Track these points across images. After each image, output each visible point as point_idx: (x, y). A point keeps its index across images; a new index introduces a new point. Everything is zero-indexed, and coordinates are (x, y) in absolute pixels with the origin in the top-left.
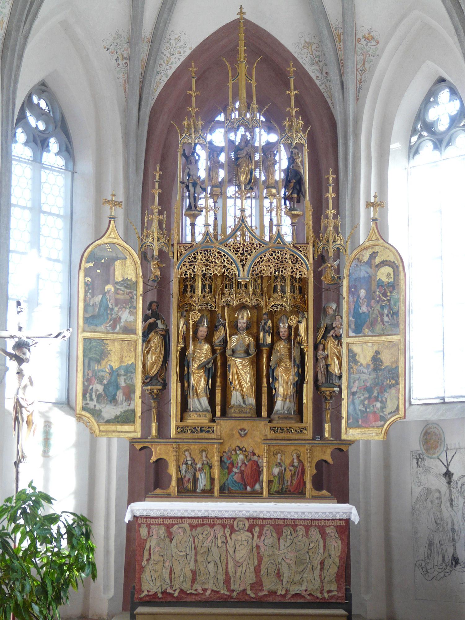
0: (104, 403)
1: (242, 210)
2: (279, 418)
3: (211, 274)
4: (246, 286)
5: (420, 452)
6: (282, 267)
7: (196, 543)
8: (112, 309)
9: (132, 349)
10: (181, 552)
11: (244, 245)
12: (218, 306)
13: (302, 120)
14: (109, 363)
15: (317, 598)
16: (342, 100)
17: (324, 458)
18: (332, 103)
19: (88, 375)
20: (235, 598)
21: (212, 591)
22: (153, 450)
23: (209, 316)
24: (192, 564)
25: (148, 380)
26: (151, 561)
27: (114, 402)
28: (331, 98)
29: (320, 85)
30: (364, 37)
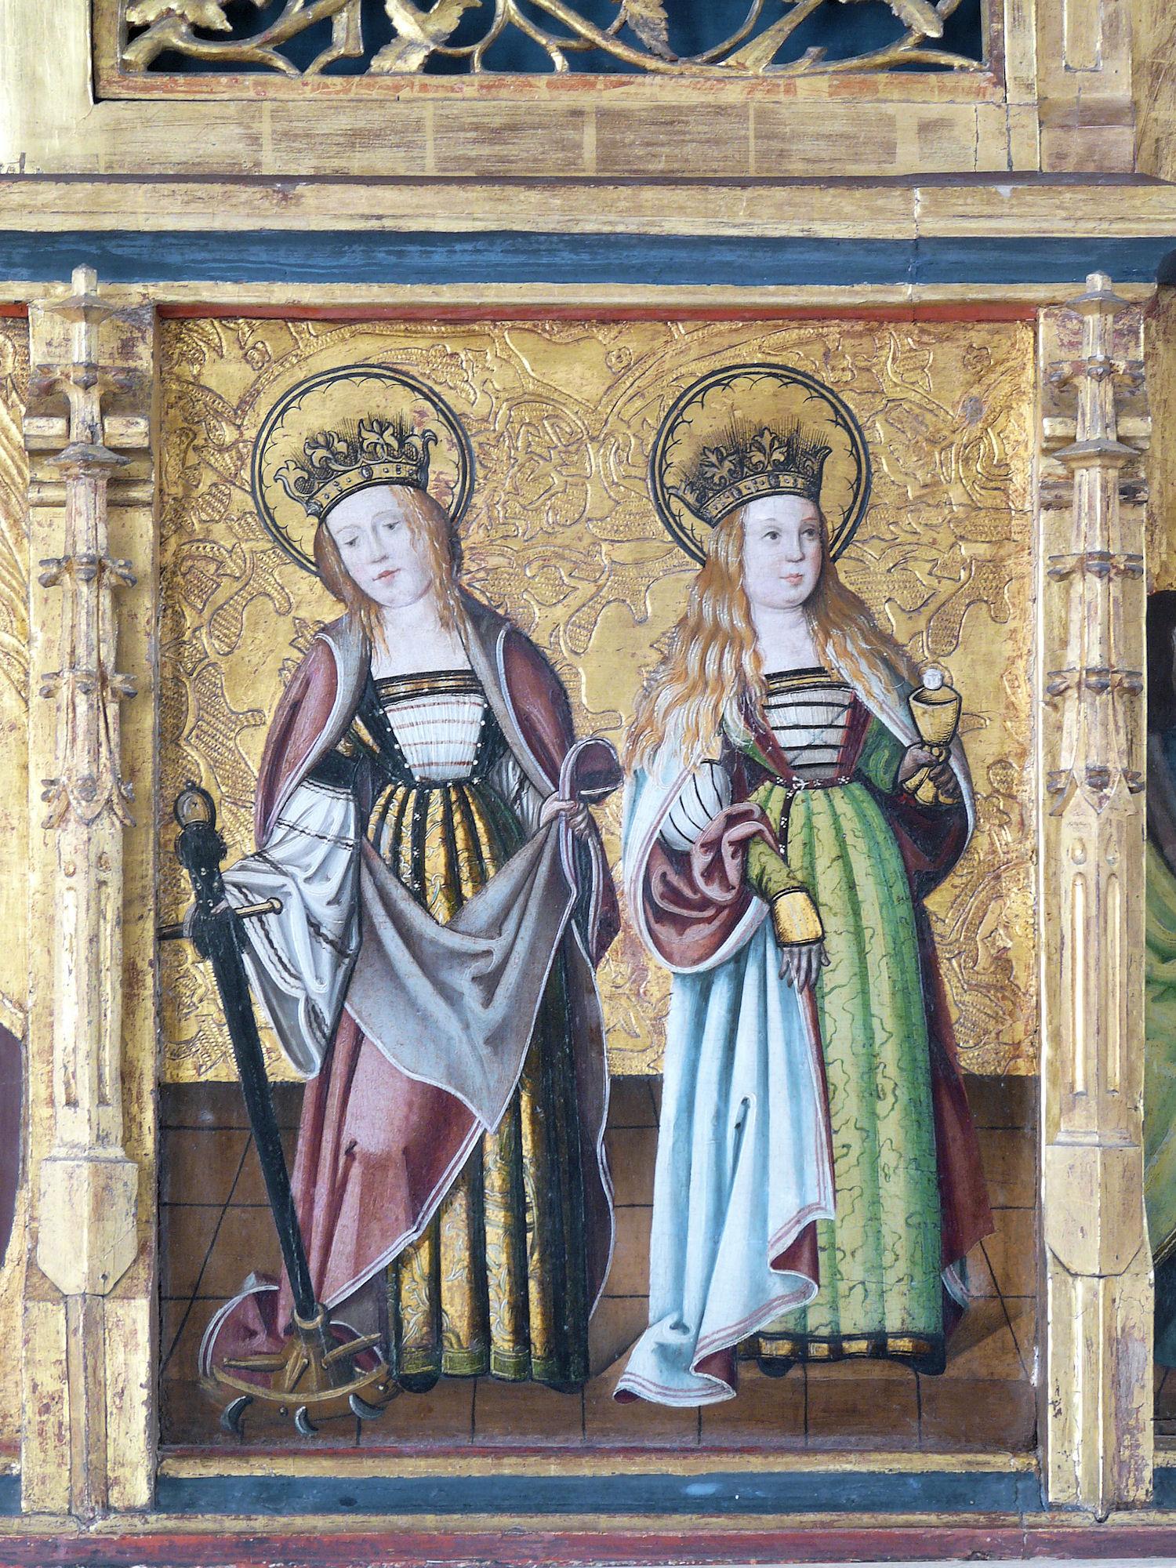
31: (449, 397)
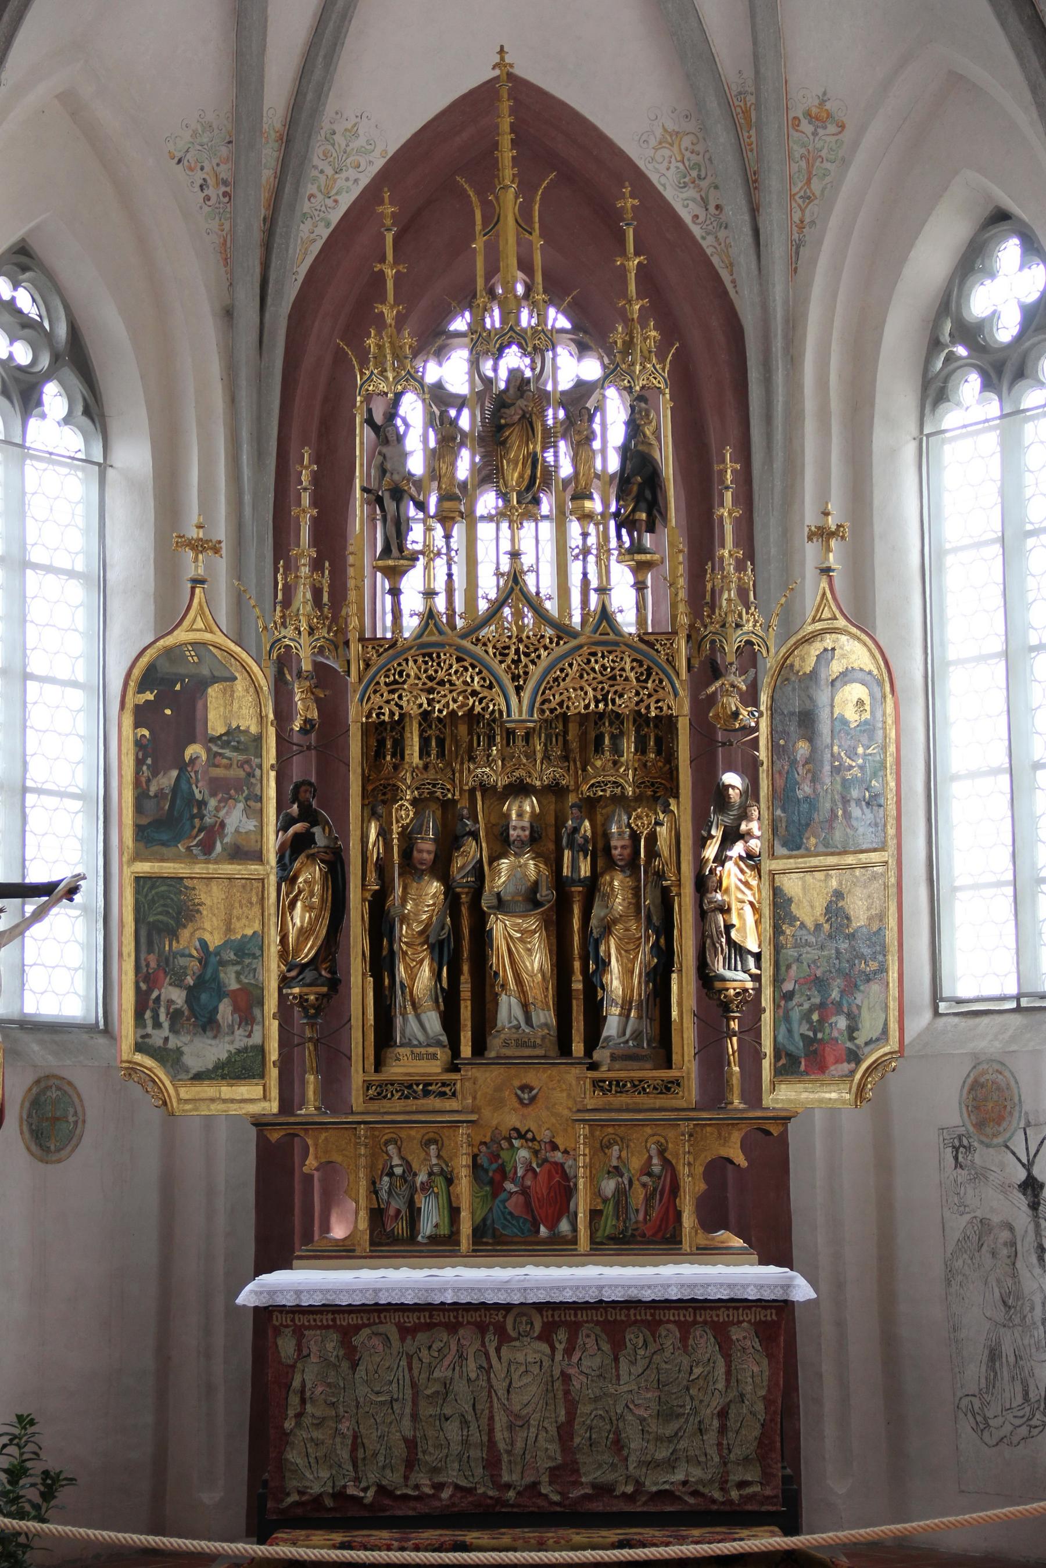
0: (188, 1032)
1: (515, 555)
2: (613, 1058)
3: (440, 711)
4: (527, 737)
5: (962, 1130)
6: (613, 689)
7: (416, 1372)
8: (202, 804)
9: (254, 899)
10: (377, 1393)
11: (520, 640)
12: (461, 790)
13: (655, 329)
14: (198, 934)
15: (714, 1501)
16: (756, 272)
17: (724, 1152)
18: (733, 282)
19: (148, 965)
20: (512, 1506)
21: (457, 1487)
22: (310, 1142)
23: (439, 813)
24: (407, 1422)
25: (293, 974)
26: (307, 1421)
27: (212, 1030)
28: (731, 266)
29: (704, 238)
30: (808, 114)
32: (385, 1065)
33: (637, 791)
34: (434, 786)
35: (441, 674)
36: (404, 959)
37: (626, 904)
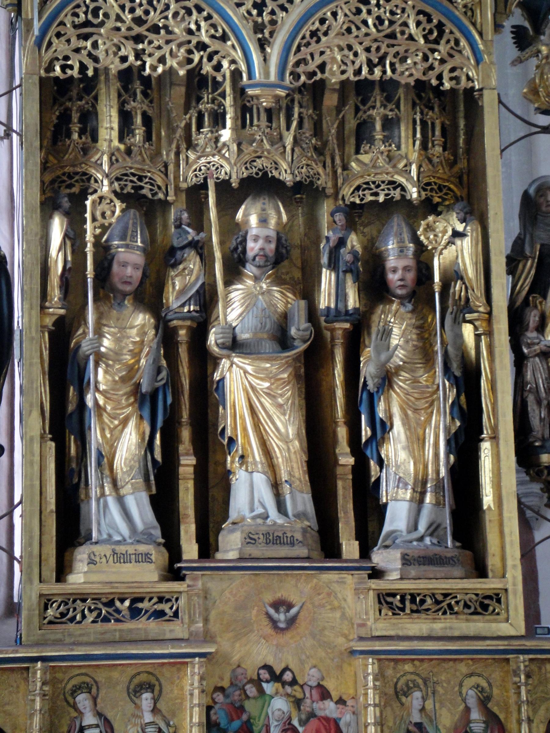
2: (406, 560)
3: (154, 68)
12: (177, 189)
31: (96, 678)
32: (71, 572)
33: (423, 193)
34: (140, 179)
35: (154, 17)
36: (100, 417)
37: (410, 347)
